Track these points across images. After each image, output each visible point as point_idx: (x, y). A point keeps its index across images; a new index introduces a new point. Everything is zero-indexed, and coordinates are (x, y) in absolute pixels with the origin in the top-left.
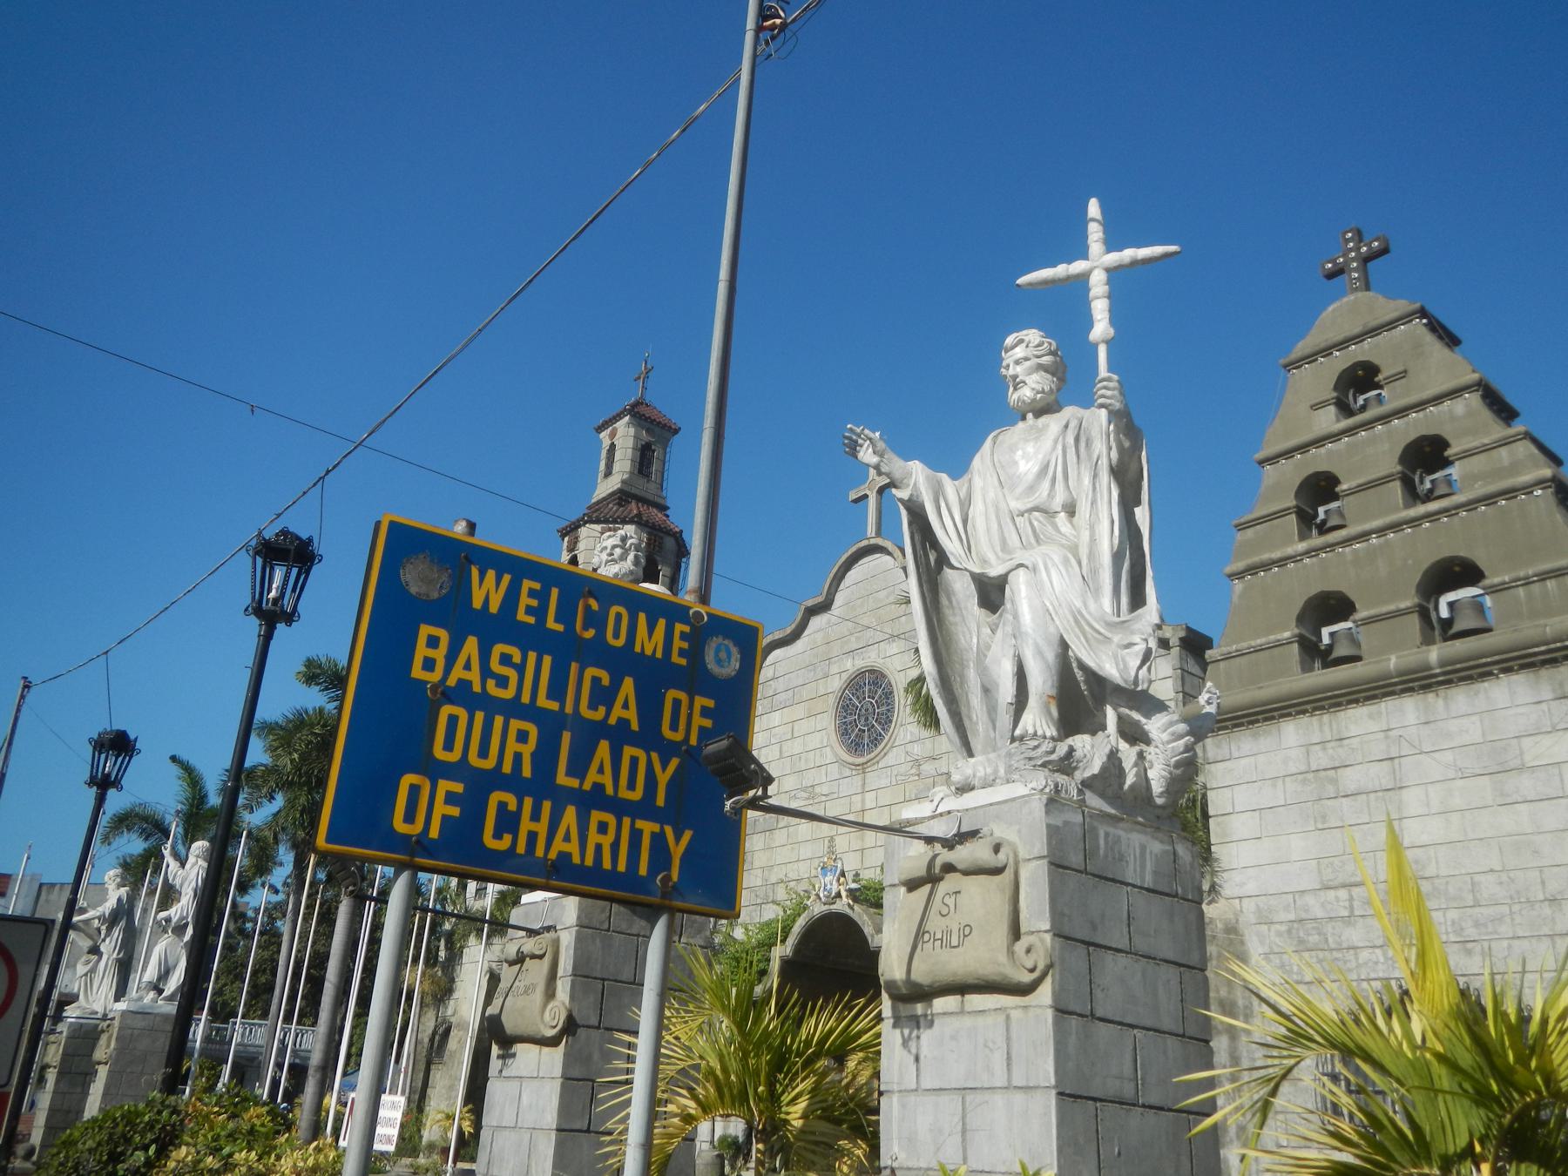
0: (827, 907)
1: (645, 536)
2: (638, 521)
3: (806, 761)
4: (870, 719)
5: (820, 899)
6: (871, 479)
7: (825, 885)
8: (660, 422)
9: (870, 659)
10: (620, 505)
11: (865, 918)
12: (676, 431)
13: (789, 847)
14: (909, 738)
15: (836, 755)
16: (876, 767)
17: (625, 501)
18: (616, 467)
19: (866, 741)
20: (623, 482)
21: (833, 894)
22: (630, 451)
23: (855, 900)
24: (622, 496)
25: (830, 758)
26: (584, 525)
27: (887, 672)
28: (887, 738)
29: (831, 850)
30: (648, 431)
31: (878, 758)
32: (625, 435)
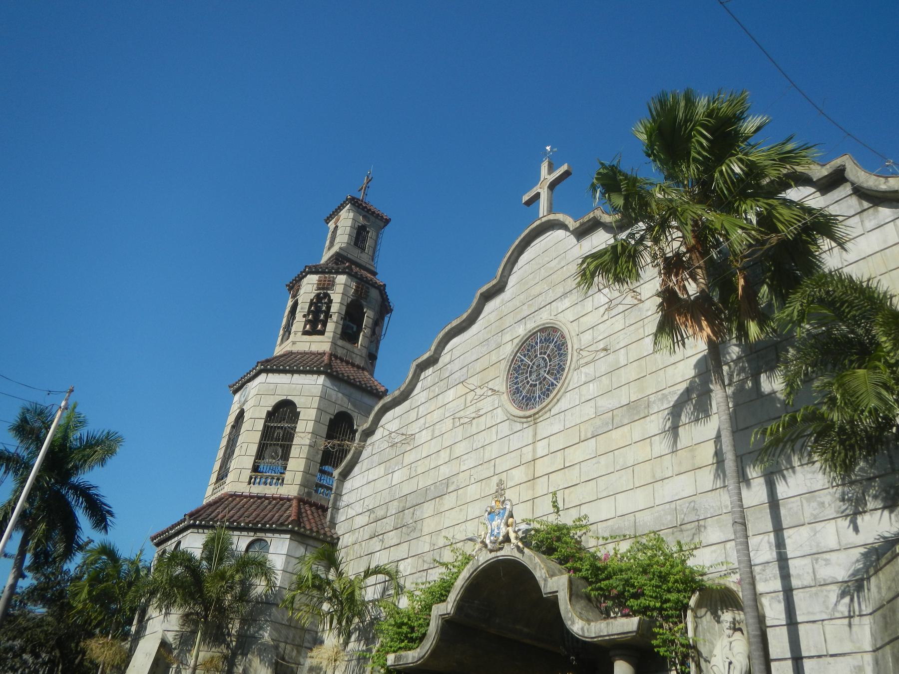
0: (493, 554)
1: (354, 285)
2: (350, 274)
3: (477, 425)
4: (542, 372)
5: (486, 546)
6: (542, 179)
7: (492, 531)
8: (374, 212)
9: (544, 318)
10: (337, 264)
11: (537, 560)
12: (387, 221)
13: (458, 509)
14: (583, 379)
15: (507, 411)
16: (548, 415)
17: (341, 261)
18: (337, 240)
19: (538, 393)
20: (340, 248)
21: (501, 538)
22: (348, 229)
23: (527, 544)
24: (339, 258)
25: (500, 415)
26: (305, 276)
27: (559, 325)
28: (559, 385)
29: (500, 491)
30: (364, 217)
31: (550, 406)
32: (346, 219)
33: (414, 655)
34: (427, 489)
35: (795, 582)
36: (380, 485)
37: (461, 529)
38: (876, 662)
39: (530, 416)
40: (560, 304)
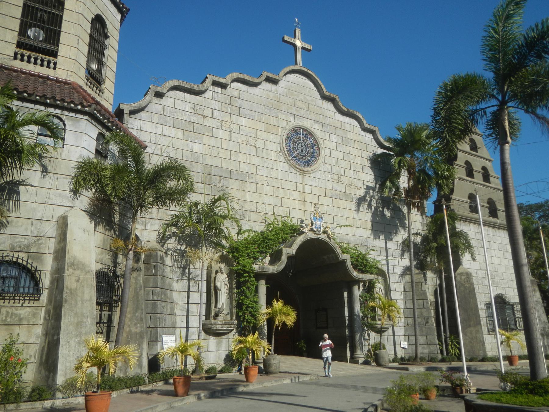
0: (316, 235)
16: (310, 175)
33: (274, 269)
34: (231, 172)
35: (390, 272)
36: (179, 144)
37: (261, 206)
38: (406, 294)
39: (303, 171)
40: (313, 123)
